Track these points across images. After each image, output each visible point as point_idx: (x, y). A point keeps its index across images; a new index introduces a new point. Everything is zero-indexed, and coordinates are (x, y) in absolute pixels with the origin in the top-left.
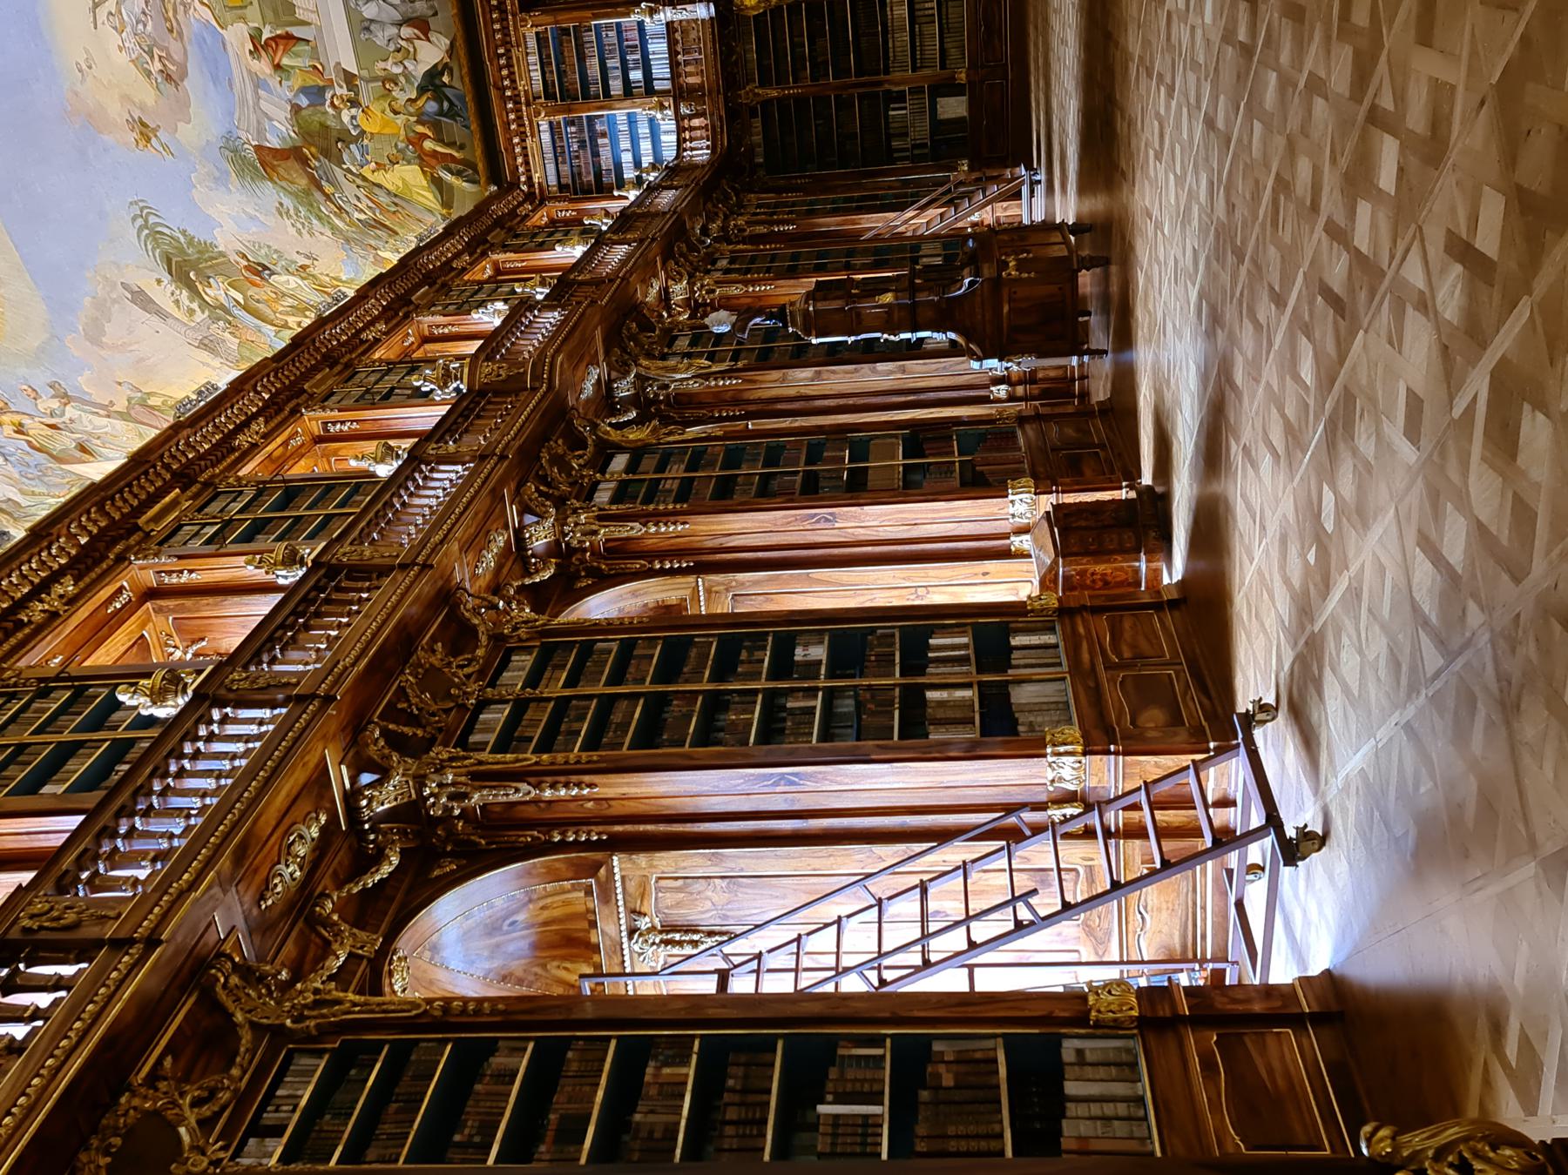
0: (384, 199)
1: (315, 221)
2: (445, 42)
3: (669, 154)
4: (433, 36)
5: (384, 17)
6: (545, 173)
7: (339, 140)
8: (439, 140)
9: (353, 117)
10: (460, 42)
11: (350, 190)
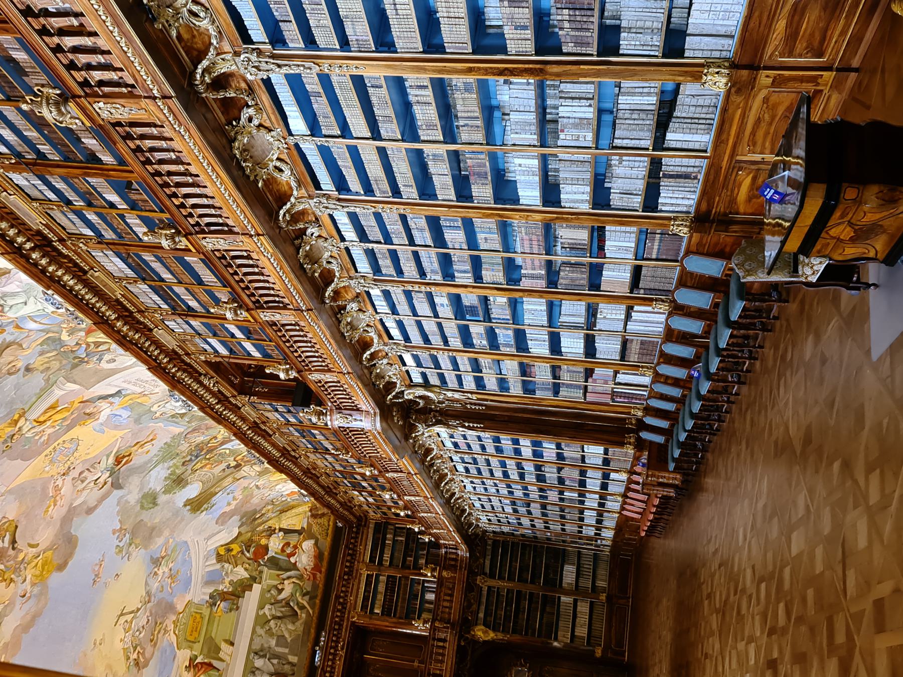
5: (265, 669)
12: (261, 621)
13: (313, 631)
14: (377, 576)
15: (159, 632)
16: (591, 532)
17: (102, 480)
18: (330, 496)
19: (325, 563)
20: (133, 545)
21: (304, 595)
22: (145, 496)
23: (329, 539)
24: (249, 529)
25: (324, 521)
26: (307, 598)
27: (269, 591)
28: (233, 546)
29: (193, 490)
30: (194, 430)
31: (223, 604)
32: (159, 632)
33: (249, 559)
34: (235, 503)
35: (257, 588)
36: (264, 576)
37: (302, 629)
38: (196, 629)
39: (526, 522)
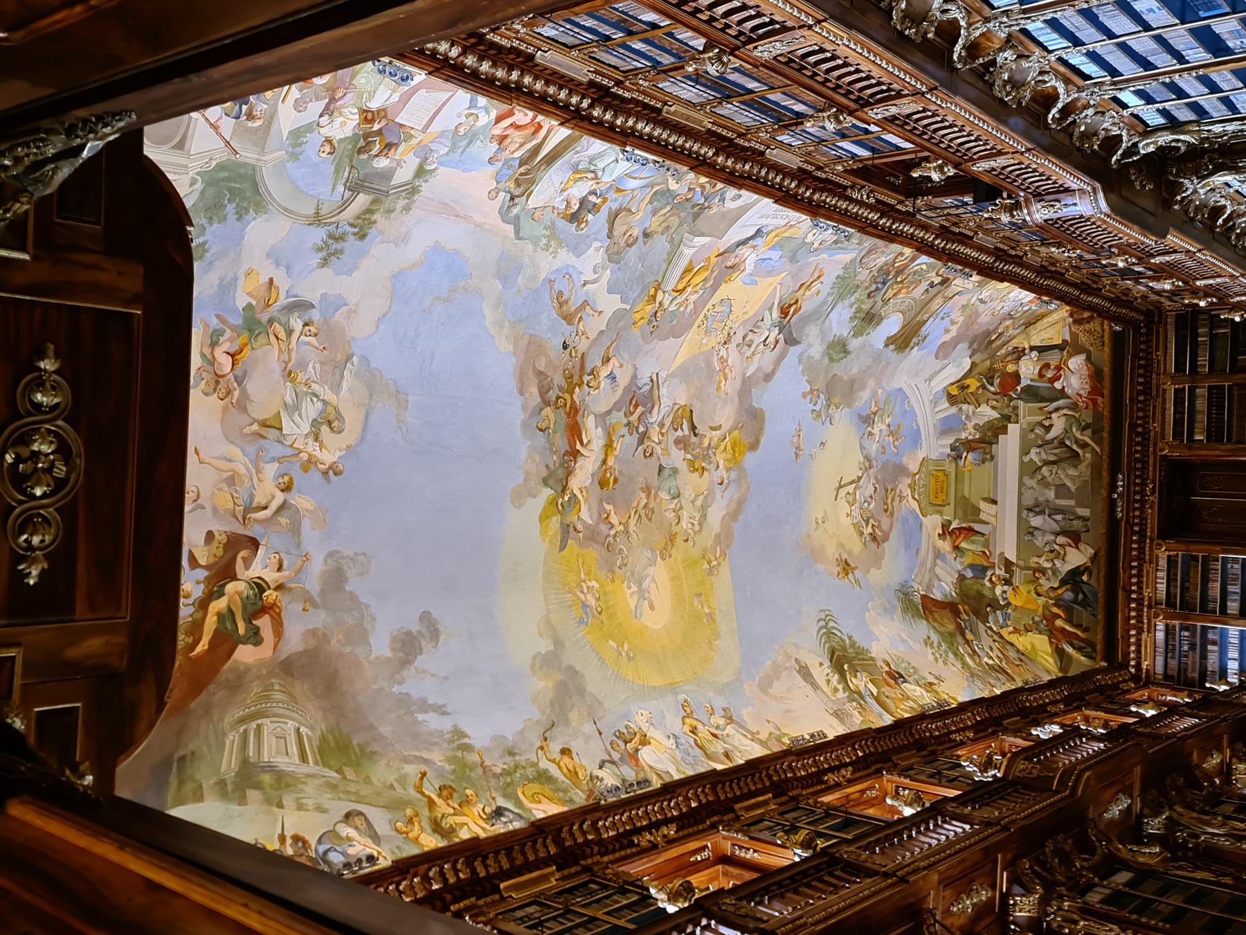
0: (1012, 654)
1: (951, 655)
2: (1091, 551)
4: (1082, 546)
5: (1046, 527)
8: (1069, 621)
9: (1004, 592)
10: (1102, 553)
11: (986, 641)
12: (1028, 470)
14: (1192, 390)
15: (893, 500)
17: (771, 339)
18: (1090, 294)
19: (1107, 383)
20: (833, 406)
21: (1084, 429)
23: (1106, 349)
24: (985, 356)
25: (1095, 325)
26: (1089, 432)
27: (1032, 430)
28: (967, 382)
29: (892, 324)
30: (869, 252)
31: (970, 456)
32: (893, 500)
33: (995, 394)
34: (954, 329)
35: (1014, 429)
36: (1021, 413)
38: (941, 489)
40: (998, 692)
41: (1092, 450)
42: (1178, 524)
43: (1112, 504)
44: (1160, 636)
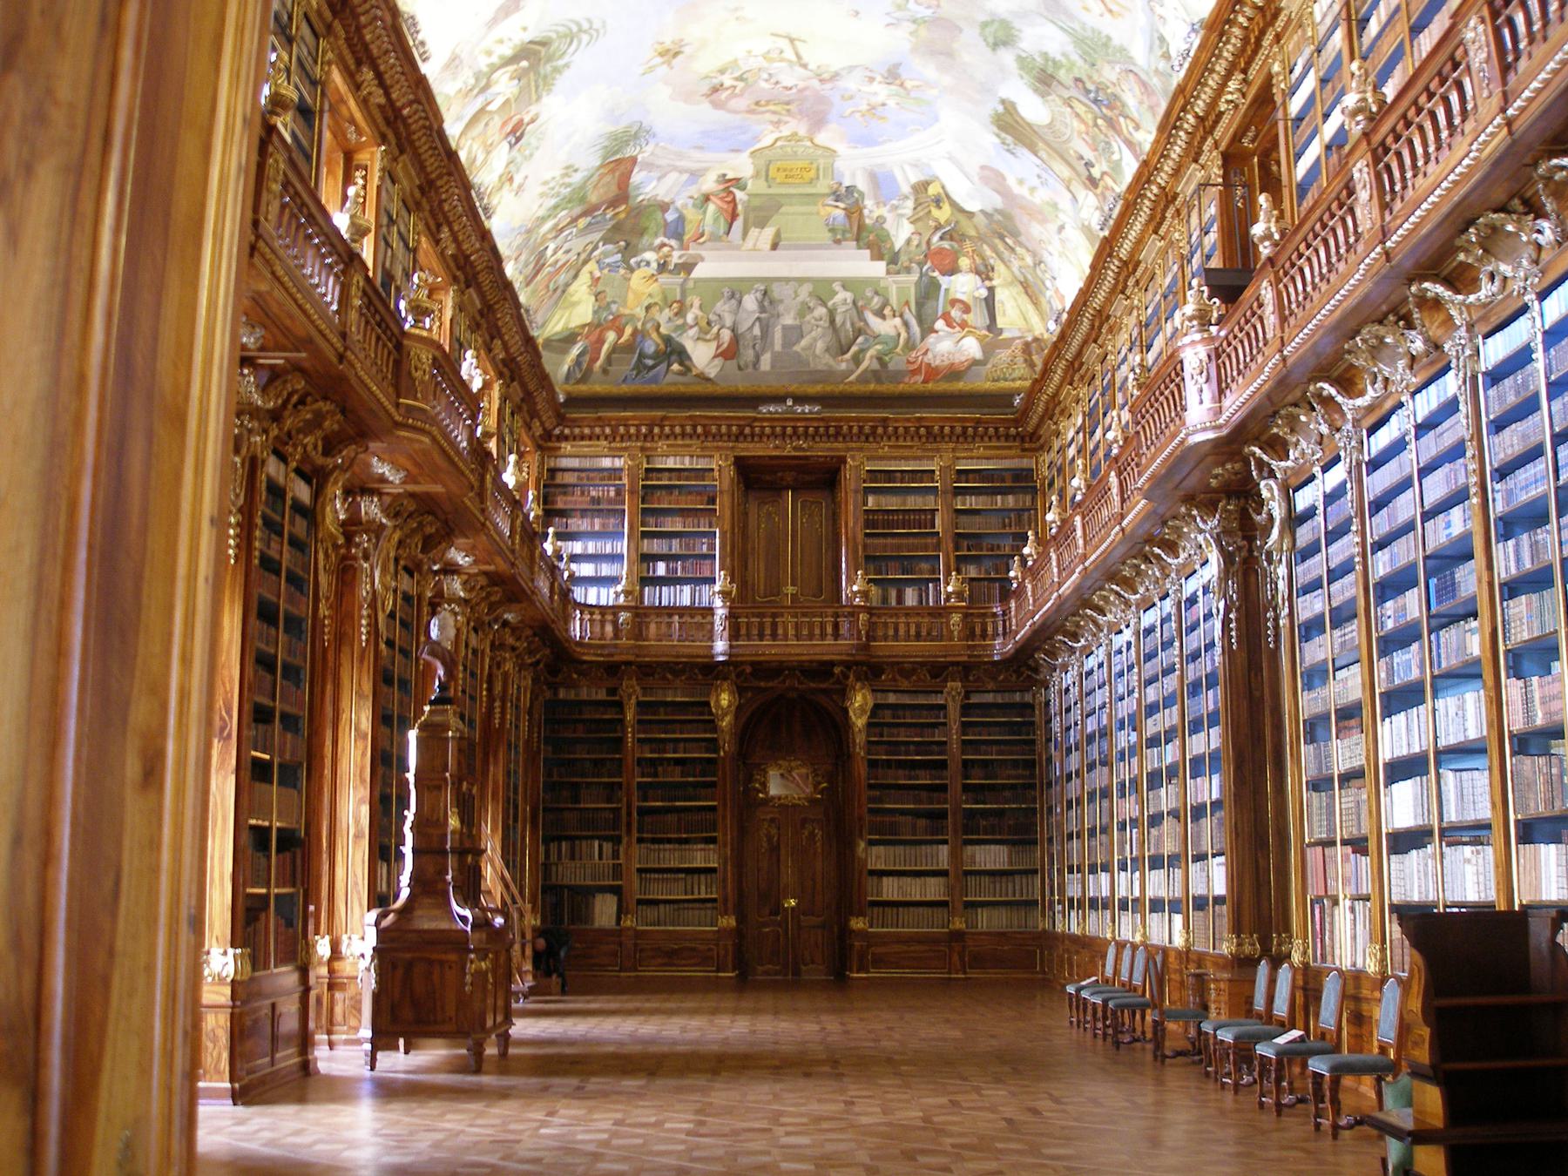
0: (562, 278)
1: (553, 202)
2: (712, 373)
3: (578, 594)
4: (719, 361)
5: (742, 315)
6: (570, 458)
7: (628, 245)
8: (615, 349)
9: (648, 264)
11: (578, 244)
12: (822, 289)
13: (818, 389)
15: (774, 113)
16: (1073, 891)
18: (1066, 372)
20: (913, 27)
21: (880, 359)
22: (1005, 25)
23: (988, 386)
24: (983, 229)
25: (1021, 369)
26: (876, 366)
27: (877, 293)
28: (946, 207)
29: (1033, 109)
30: (1144, 84)
31: (839, 213)
32: (774, 113)
33: (928, 243)
35: (879, 269)
36: (902, 277)
37: (820, 367)
38: (789, 175)
39: (1074, 762)
40: (510, 270)
41: (850, 371)
42: (755, 478)
43: (779, 399)
44: (606, 463)
